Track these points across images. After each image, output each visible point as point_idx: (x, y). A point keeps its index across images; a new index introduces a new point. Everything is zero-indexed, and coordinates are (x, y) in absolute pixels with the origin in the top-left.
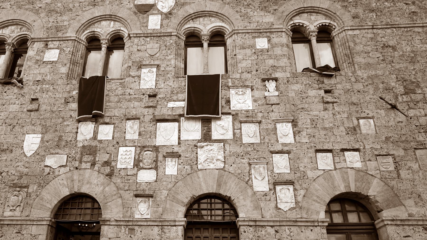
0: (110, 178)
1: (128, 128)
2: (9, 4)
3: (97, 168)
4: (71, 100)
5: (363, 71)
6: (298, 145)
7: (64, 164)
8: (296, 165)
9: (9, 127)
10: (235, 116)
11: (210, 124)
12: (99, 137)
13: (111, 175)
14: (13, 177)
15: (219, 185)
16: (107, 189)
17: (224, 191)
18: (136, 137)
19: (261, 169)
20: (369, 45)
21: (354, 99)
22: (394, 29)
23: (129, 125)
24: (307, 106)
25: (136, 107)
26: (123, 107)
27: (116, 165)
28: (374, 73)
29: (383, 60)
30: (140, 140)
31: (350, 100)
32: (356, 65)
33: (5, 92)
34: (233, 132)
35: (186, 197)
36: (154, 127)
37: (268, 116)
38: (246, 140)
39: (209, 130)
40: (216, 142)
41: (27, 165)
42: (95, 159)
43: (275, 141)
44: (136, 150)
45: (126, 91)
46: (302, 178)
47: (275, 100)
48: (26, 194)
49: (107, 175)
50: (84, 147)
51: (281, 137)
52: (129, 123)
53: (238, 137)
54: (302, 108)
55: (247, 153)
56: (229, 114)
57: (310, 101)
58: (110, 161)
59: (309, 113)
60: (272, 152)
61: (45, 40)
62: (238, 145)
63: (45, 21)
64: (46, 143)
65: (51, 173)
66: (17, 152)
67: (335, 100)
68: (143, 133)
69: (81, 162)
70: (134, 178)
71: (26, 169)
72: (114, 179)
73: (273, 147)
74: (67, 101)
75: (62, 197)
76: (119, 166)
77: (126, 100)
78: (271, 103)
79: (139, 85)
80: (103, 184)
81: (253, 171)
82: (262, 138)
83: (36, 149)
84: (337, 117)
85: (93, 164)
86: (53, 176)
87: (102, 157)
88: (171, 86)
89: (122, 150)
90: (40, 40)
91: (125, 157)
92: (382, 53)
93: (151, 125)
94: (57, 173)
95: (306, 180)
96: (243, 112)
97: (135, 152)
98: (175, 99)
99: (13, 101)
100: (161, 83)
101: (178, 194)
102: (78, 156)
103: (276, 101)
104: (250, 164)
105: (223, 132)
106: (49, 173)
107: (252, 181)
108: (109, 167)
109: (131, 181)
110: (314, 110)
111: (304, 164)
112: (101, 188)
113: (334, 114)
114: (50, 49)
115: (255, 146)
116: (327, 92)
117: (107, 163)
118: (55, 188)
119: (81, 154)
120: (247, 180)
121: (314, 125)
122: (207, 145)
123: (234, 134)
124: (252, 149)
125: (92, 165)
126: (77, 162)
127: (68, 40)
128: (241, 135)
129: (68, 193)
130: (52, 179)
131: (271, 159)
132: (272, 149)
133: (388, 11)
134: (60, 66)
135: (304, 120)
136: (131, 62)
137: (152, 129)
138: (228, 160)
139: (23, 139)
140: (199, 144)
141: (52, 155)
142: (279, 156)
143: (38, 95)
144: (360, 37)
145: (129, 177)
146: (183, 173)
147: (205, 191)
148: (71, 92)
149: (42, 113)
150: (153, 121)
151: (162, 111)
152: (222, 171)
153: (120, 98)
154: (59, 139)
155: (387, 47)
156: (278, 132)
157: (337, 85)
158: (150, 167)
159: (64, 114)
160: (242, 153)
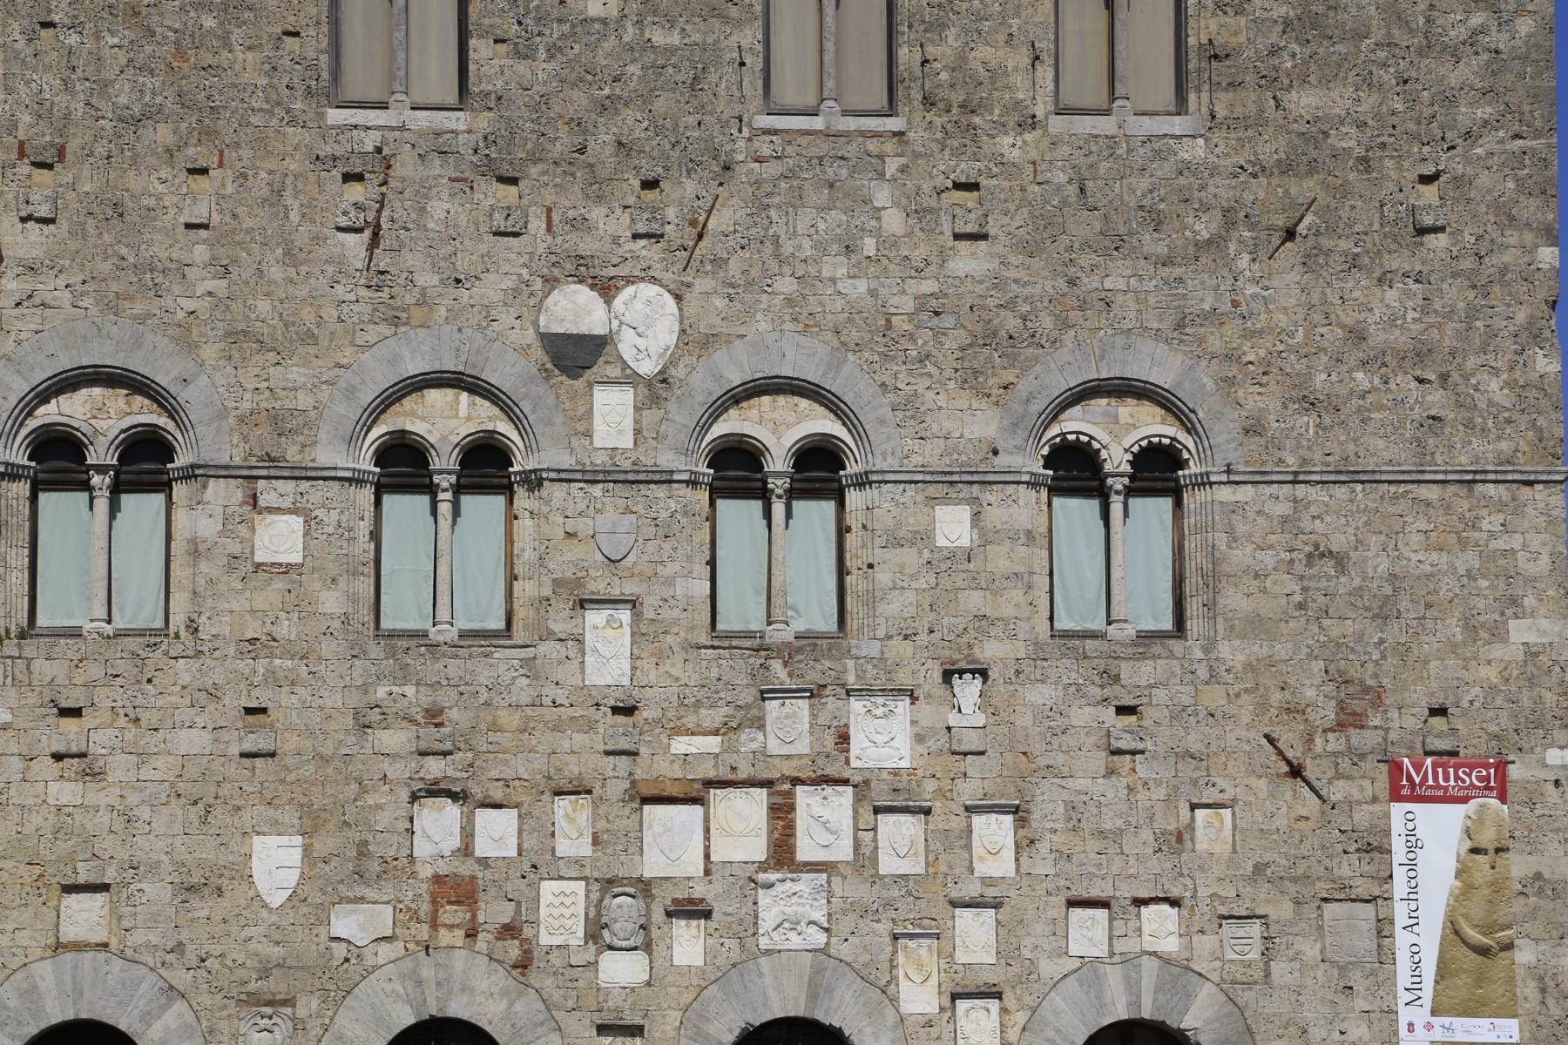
0: (523, 975)
1: (561, 823)
2: (61, 283)
3: (485, 945)
4: (374, 715)
5: (1236, 643)
6: (1025, 882)
7: (389, 933)
9: (193, 809)
10: (862, 788)
12: (479, 852)
13: (525, 967)
14: (241, 973)
15: (813, 996)
16: (518, 1006)
17: (827, 1013)
18: (585, 849)
19: (924, 952)
20: (1271, 547)
21: (1194, 742)
22: (1359, 487)
23: (562, 812)
24: (1060, 759)
25: (581, 752)
26: (540, 748)
27: (536, 936)
28: (1264, 652)
29: (1301, 606)
30: (598, 859)
31: (1183, 744)
32: (1220, 620)
33: (149, 681)
34: (855, 838)
36: (636, 817)
40: (808, 872)
41: (277, 937)
42: (474, 916)
44: (588, 891)
45: (545, 691)
47: (972, 741)
48: (290, 1024)
49: (515, 967)
50: (438, 879)
51: (981, 859)
52: (563, 805)
55: (889, 904)
56: (845, 782)
57: (1073, 743)
58: (517, 924)
60: (955, 904)
61: (245, 472)
63: (224, 381)
64: (322, 865)
65: (353, 961)
66: (236, 895)
67: (1140, 746)
68: (605, 837)
69: (434, 926)
70: (590, 974)
71: (276, 949)
72: (534, 978)
74: (366, 721)
75: (397, 1031)
76: (545, 939)
77: (546, 723)
78: (963, 748)
79: (583, 672)
80: (505, 993)
81: (901, 958)
83: (294, 884)
84: (1139, 797)
85: (471, 934)
86: (360, 969)
87: (495, 912)
88: (678, 679)
89: (548, 888)
90: (225, 472)
91: (560, 911)
92: (1302, 578)
93: (627, 811)
94: (370, 961)
96: (885, 775)
97: (587, 896)
98: (690, 726)
99: (184, 717)
100: (647, 667)
101: (708, 1020)
102: (425, 908)
103: (977, 742)
105: (825, 838)
106: (347, 960)
108: (516, 942)
109: (581, 984)
110: (1081, 774)
112: (503, 1005)
113: (1130, 789)
114: (271, 510)
115: (911, 884)
116: (1122, 710)
117: (509, 931)
118: (373, 1006)
119: (434, 902)
120: (884, 982)
121: (1074, 822)
123: (857, 846)
125: (468, 936)
126: (425, 927)
127: (325, 479)
128: (876, 848)
129: (411, 1021)
130: (358, 978)
131: (950, 923)
132: (954, 895)
133: (1359, 410)
134: (317, 586)
135: (1048, 804)
136: (547, 580)
137: (631, 823)
139: (245, 850)
140: (762, 877)
141: (350, 906)
144: (1250, 512)
146: (720, 961)
148: (371, 690)
149: (290, 761)
150: (632, 799)
151: (655, 766)
153: (528, 718)
154: (361, 854)
155: (1322, 555)
157: (1154, 691)
158: (631, 943)
159: (360, 766)
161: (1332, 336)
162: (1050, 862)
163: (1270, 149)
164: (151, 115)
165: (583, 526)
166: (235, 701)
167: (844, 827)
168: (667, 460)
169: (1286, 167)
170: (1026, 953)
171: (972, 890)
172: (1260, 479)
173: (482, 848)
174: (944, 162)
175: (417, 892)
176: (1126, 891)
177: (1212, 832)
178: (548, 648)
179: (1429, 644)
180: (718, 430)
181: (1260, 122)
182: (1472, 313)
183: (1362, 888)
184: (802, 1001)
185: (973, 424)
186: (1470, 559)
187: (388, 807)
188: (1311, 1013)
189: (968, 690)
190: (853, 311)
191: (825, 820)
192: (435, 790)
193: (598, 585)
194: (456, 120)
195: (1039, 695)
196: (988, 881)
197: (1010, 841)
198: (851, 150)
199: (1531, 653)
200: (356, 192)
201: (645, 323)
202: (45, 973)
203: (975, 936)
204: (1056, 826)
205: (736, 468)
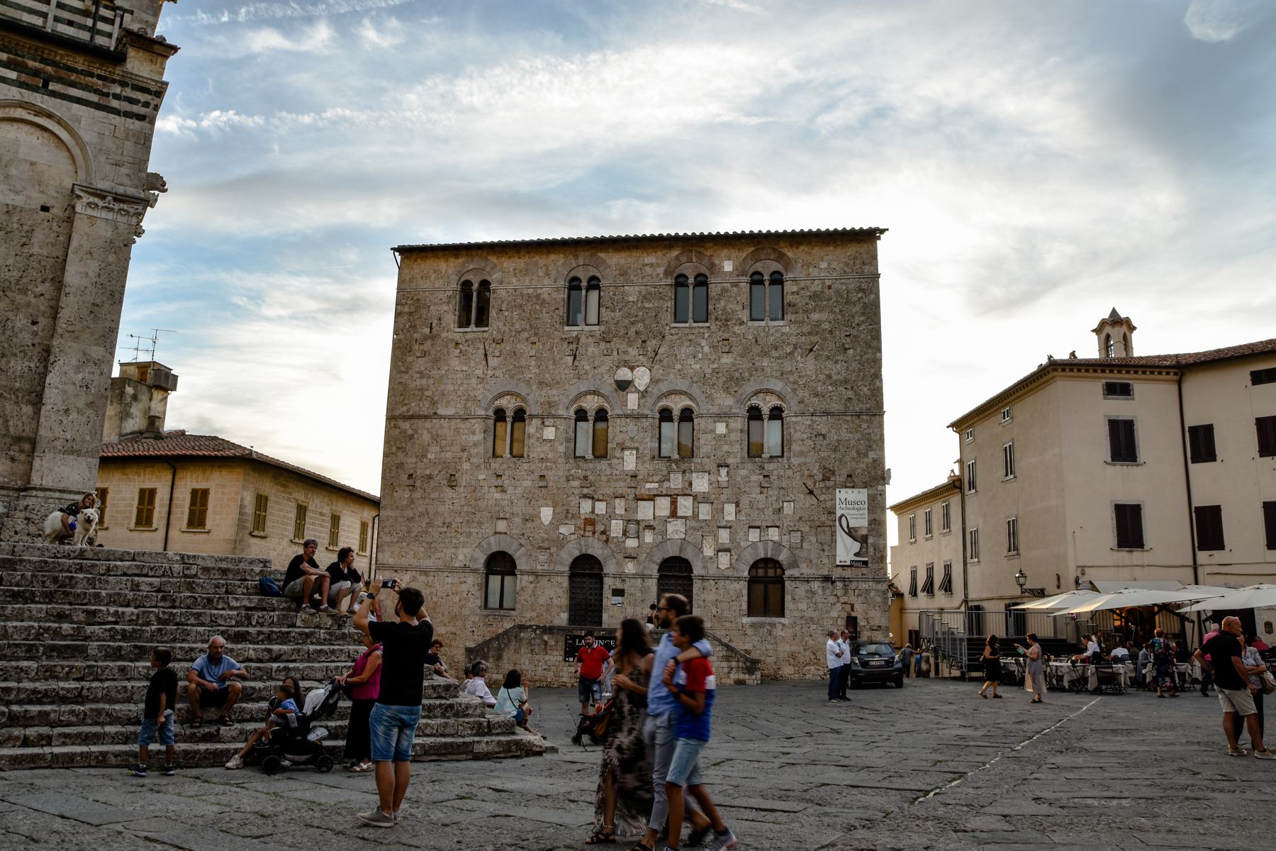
10: (695, 497)
15: (681, 551)
18: (623, 512)
25: (621, 487)
35: (659, 558)
38: (702, 517)
47: (725, 485)
52: (617, 501)
87: (600, 528)
90: (537, 416)
91: (616, 527)
117: (603, 532)
135: (745, 501)
143: (544, 473)
145: (620, 544)
147: (671, 554)
161: (822, 377)
163: (805, 330)
164: (524, 330)
165: (624, 429)
166: (537, 473)
168: (646, 412)
169: (810, 334)
171: (724, 524)
172: (803, 414)
173: (597, 511)
174: (720, 333)
175: (581, 522)
176: (764, 524)
177: (788, 508)
178: (614, 461)
179: (847, 459)
180: (660, 404)
181: (803, 322)
182: (860, 370)
183: (829, 523)
185: (727, 401)
186: (859, 435)
187: (574, 500)
188: (813, 556)
189: (724, 471)
190: (696, 373)
191: (685, 506)
192: (585, 496)
193: (628, 444)
194: (596, 328)
195: (743, 472)
198: (696, 331)
199: (875, 460)
200: (571, 346)
201: (642, 377)
202: (492, 539)
203: (724, 536)
205: (666, 415)
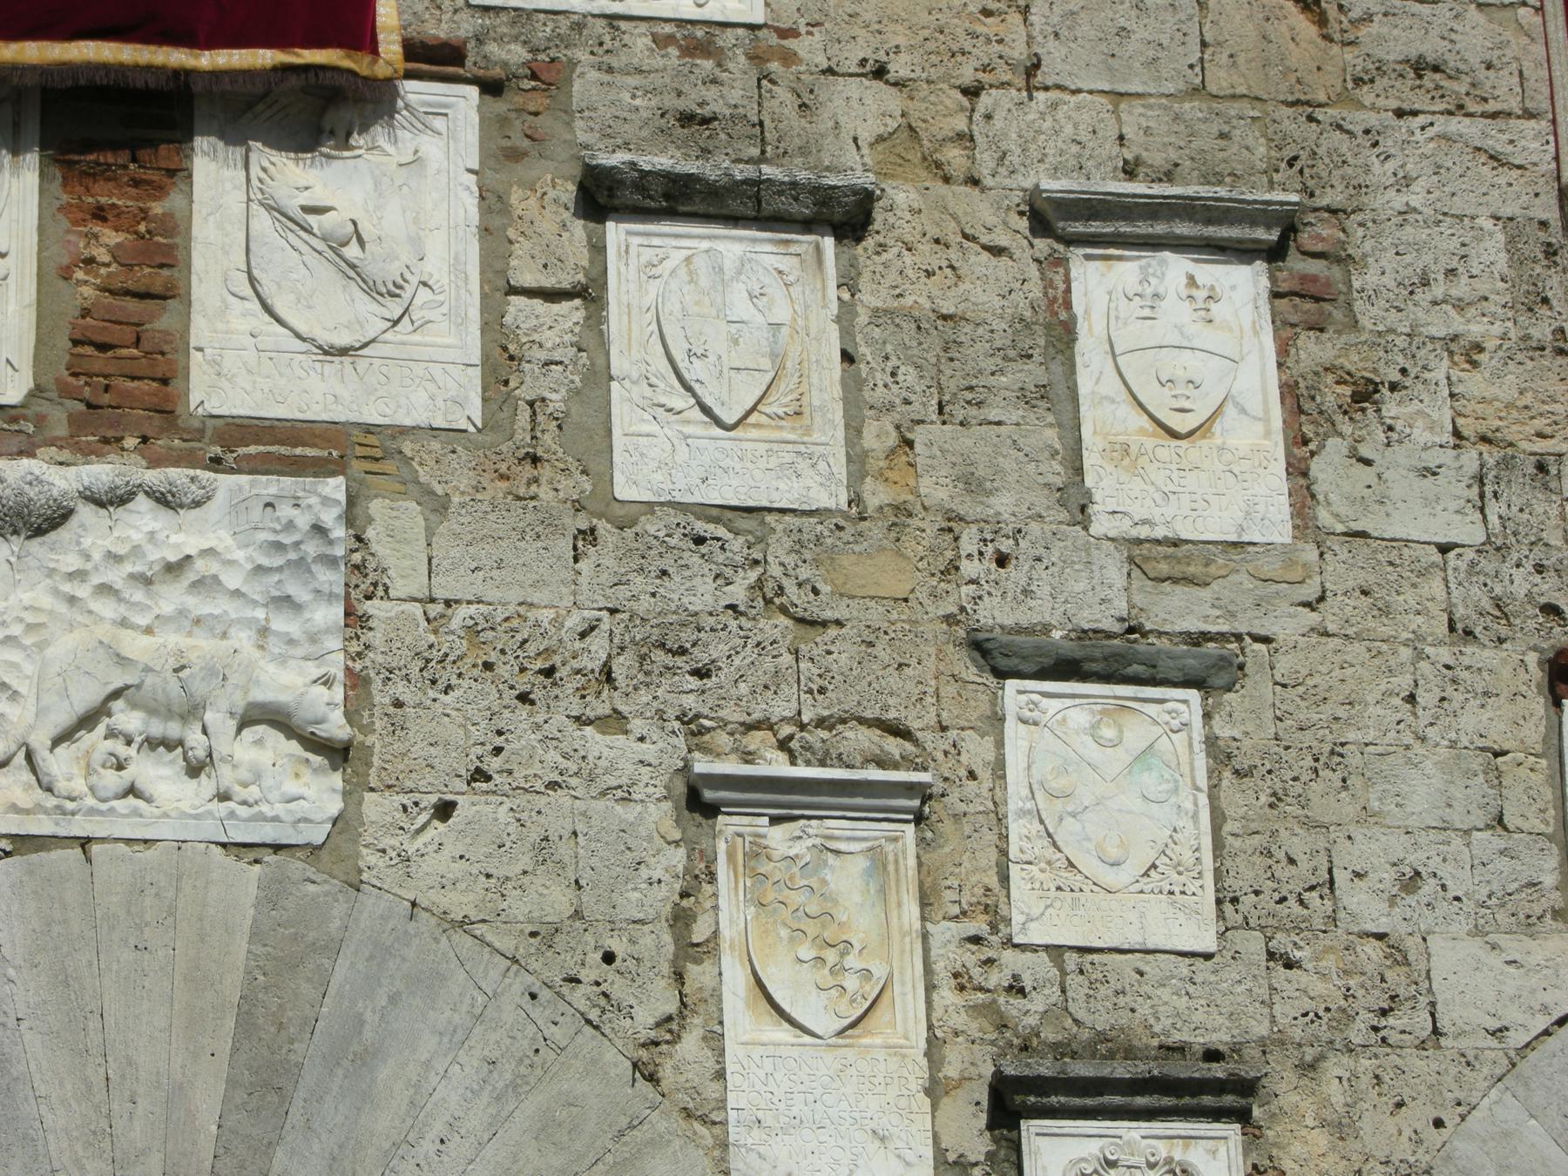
6: (1343, 570)
8: (1297, 843)
11: (159, 191)
19: (847, 880)
34: (493, 323)
37: (965, 139)
38: (656, 456)
39: (144, 276)
43: (1041, 501)
46: (1358, 1033)
51: (1122, 452)
53: (556, 401)
54: (1420, 67)
55: (671, 646)
59: (1498, 143)
62: (550, 523)
73: (1015, 575)
81: (729, 910)
82: (878, 436)
95: (1416, 1062)
96: (640, 41)
104: (699, 802)
105: (339, 312)
107: (715, 1040)
111: (1397, 845)
115: (779, 552)
120: (644, 1019)
122: (112, 500)
123: (502, 361)
124: (738, 592)
131: (977, 750)
132: (995, 614)
138: (397, 728)
142: (1079, 717)
152: (318, 888)
156: (1092, 373)
160: (599, 647)
162: (1455, 488)
167: (435, 268)
170: (1365, 905)
184: (207, 1102)
196: (1160, 558)
197: (1255, 377)
203: (1108, 822)
204: (1477, 330)
